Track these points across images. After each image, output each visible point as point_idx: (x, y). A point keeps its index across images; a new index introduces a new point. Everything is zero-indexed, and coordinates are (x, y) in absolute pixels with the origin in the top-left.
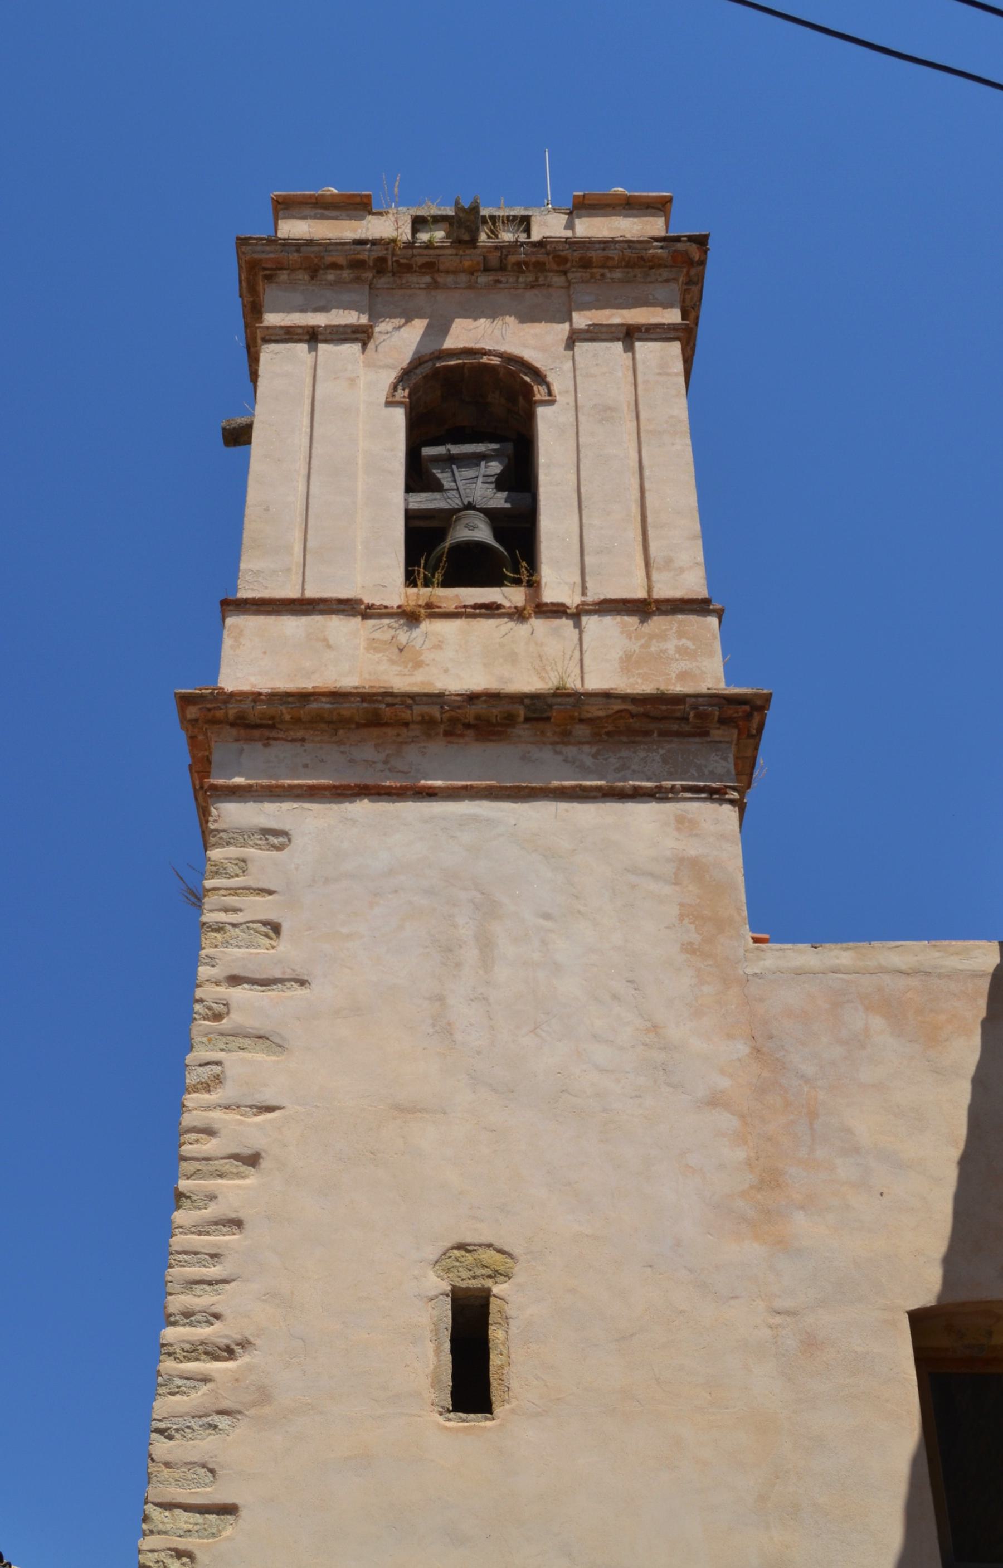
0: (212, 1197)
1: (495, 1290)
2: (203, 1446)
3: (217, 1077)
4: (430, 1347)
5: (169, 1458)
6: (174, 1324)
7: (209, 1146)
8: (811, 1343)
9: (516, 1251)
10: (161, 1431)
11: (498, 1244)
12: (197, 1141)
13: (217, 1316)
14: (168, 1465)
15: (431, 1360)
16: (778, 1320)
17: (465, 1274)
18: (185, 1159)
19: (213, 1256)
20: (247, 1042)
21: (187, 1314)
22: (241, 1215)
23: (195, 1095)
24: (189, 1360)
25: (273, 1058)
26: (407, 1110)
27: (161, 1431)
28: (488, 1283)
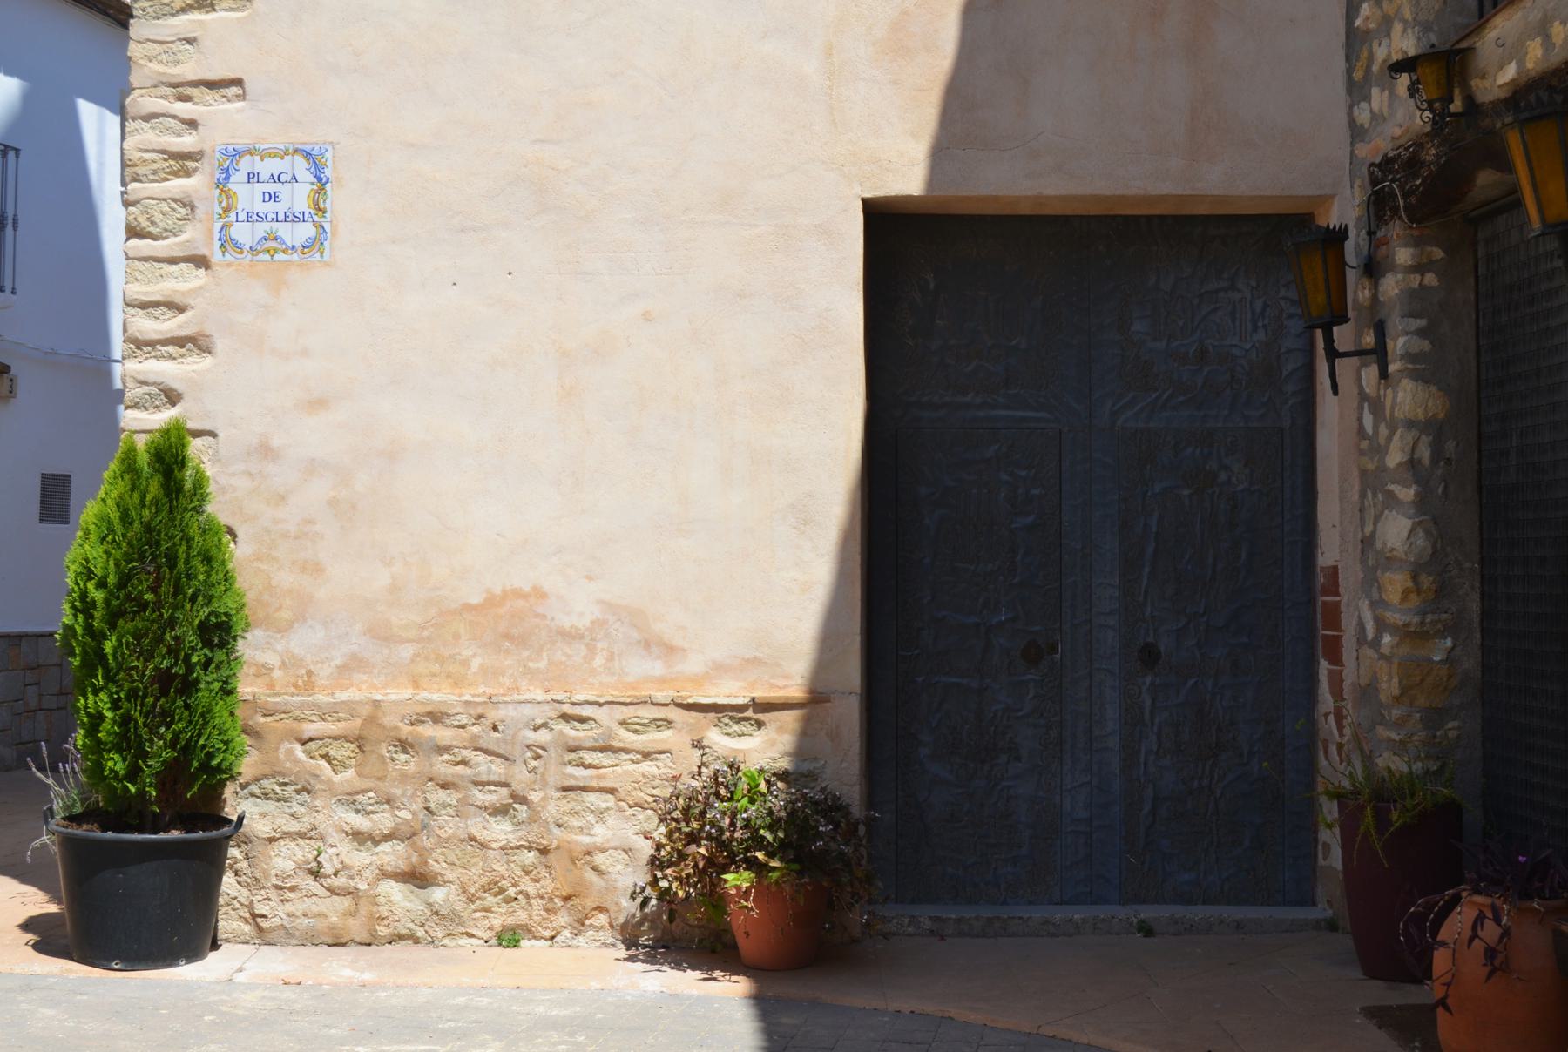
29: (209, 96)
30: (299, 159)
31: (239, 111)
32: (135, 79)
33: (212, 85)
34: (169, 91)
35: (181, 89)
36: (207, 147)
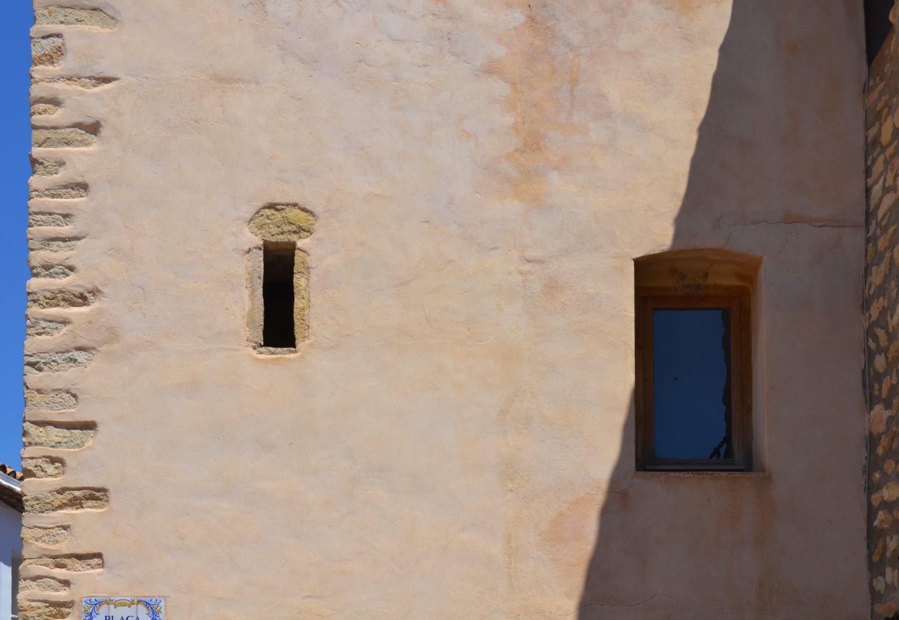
0: (61, 164)
1: (299, 244)
2: (67, 376)
3: (59, 49)
4: (246, 293)
5: (40, 386)
6: (37, 275)
7: (56, 116)
8: (552, 287)
9: (317, 210)
10: (32, 365)
11: (302, 204)
12: (45, 111)
13: (71, 269)
14: (39, 391)
15: (247, 304)
16: (528, 267)
17: (275, 230)
18: (36, 128)
19: (66, 216)
20: (84, 14)
21: (47, 267)
22: (87, 179)
23: (40, 67)
24: (51, 306)
25: (107, 30)
26: (225, 80)
27: (32, 365)
28: (294, 238)
29: (78, 564)
30: (141, 608)
31: (99, 574)
32: (25, 553)
33: (80, 557)
34: (50, 561)
35: (59, 561)
36: (76, 599)
